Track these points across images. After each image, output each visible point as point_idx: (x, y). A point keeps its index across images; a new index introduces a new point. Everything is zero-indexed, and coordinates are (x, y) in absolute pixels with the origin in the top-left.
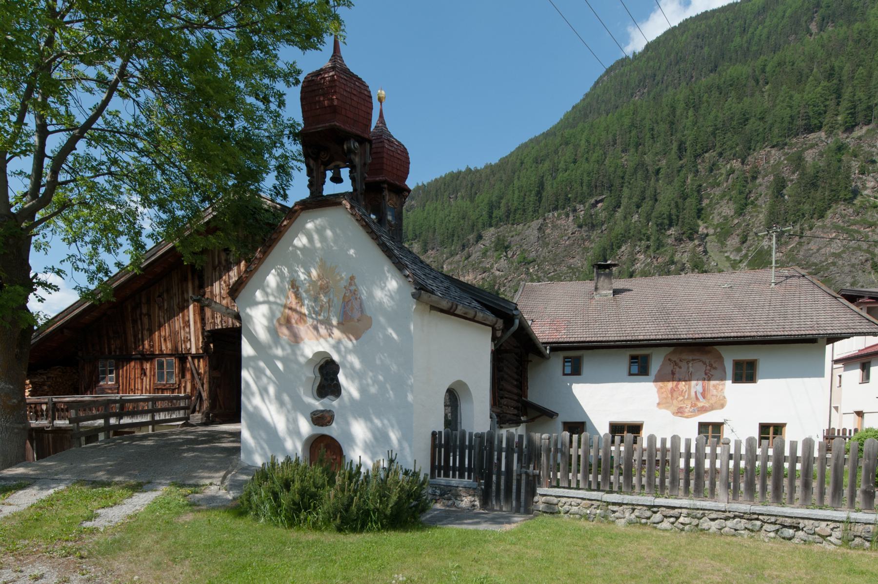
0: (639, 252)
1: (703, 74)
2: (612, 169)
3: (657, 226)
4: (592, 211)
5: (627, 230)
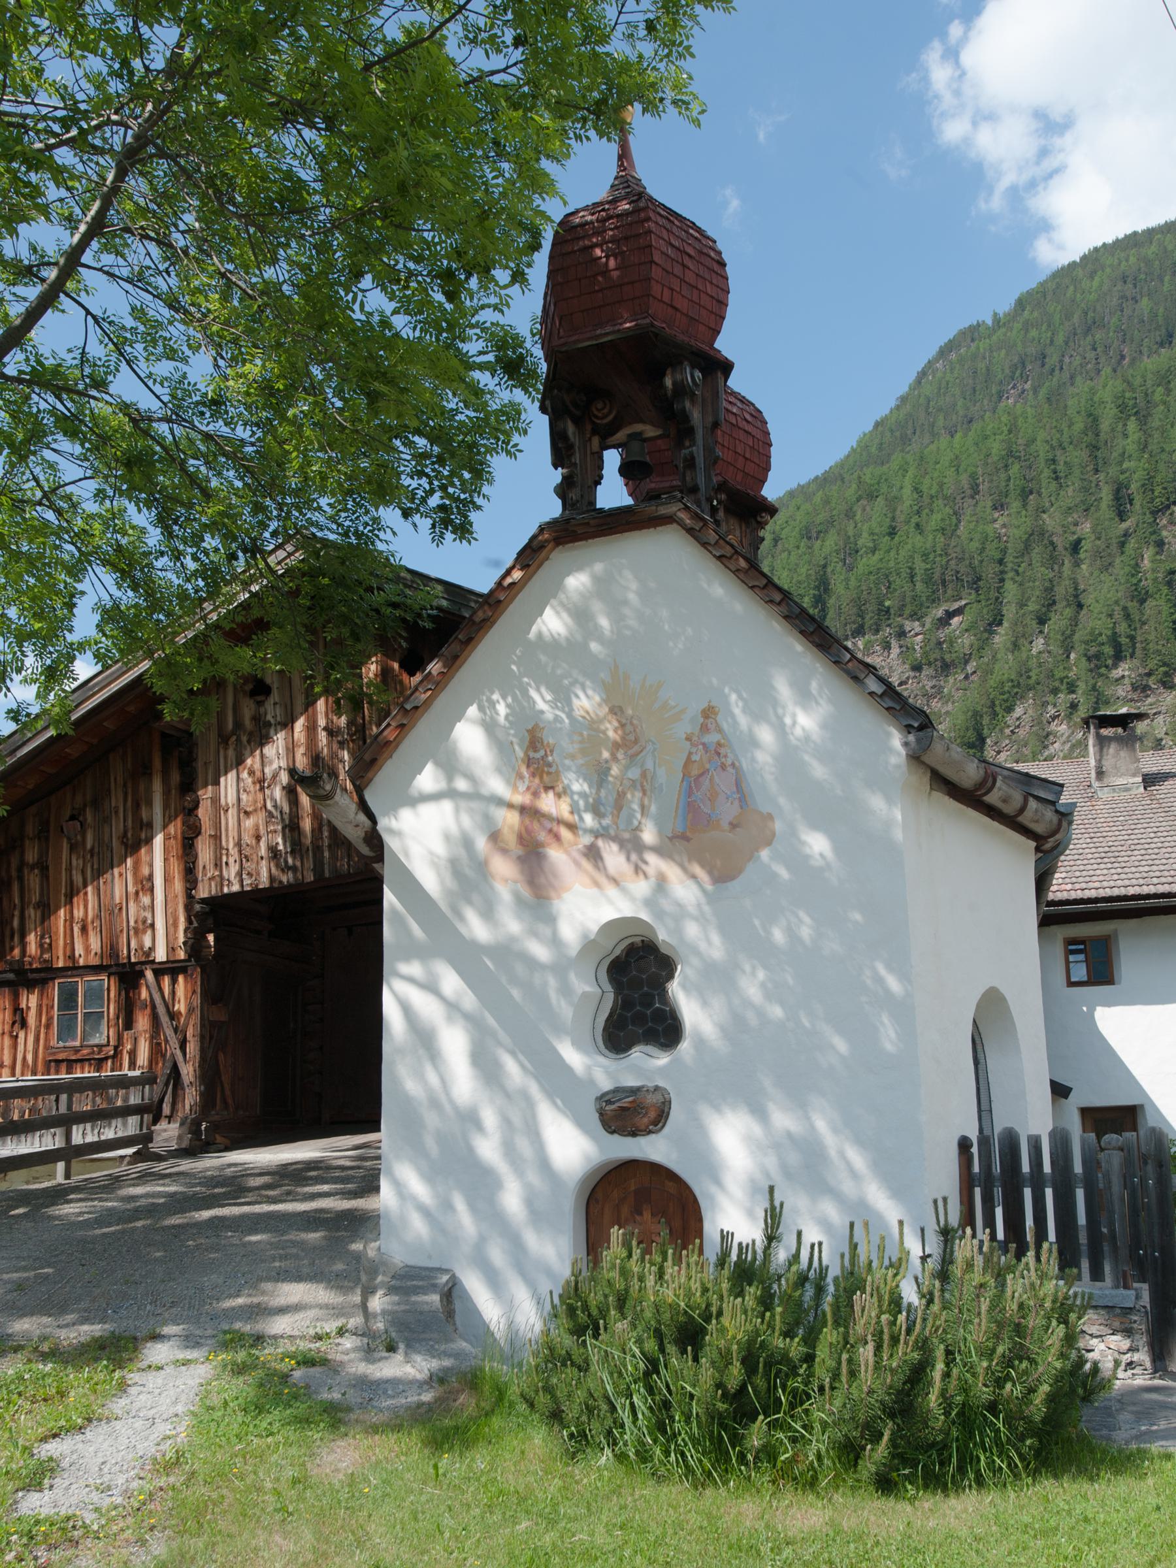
0: (1054, 718)
1: (1145, 350)
2: (975, 545)
3: (1089, 659)
4: (942, 634)
5: (1025, 672)
